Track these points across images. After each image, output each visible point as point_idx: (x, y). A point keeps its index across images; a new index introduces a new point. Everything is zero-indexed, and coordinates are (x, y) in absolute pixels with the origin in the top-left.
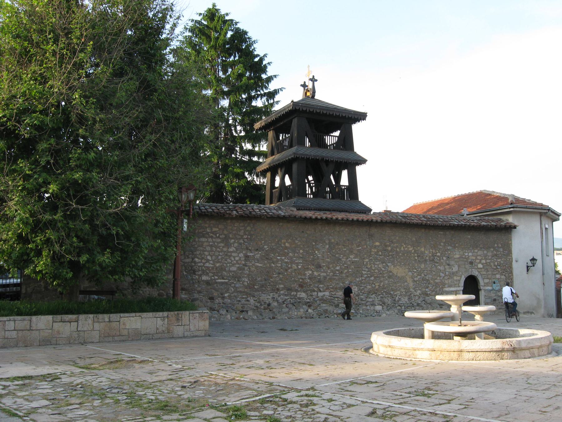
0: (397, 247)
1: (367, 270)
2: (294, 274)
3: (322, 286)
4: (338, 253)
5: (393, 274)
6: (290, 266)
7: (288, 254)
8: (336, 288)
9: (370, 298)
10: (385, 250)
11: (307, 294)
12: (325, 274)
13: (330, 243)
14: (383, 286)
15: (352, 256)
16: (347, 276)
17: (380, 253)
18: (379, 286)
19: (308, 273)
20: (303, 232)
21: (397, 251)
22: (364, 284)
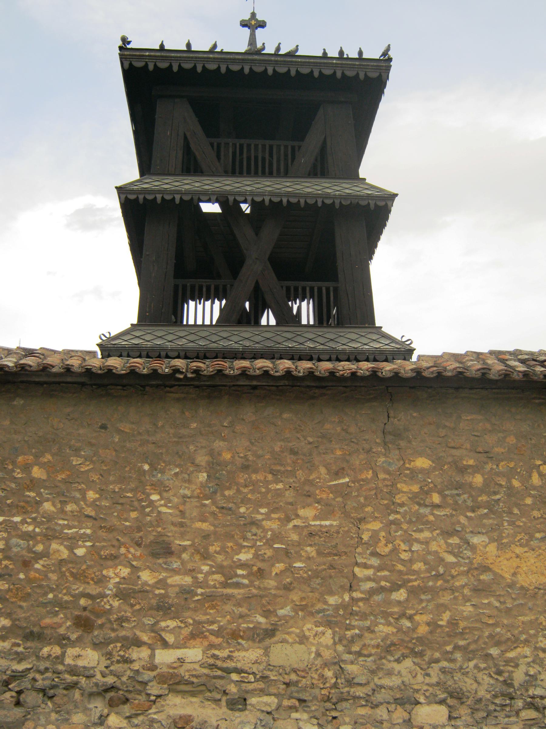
0: (510, 474)
1: (374, 561)
2: (54, 577)
3: (172, 624)
4: (245, 501)
5: (498, 578)
6: (40, 548)
7: (39, 504)
8: (235, 635)
9: (390, 673)
10: (459, 486)
11: (109, 656)
12: (188, 580)
13: (214, 467)
14: (452, 623)
15: (307, 513)
16: (288, 588)
17: (436, 498)
18: (433, 625)
19: (118, 573)
20: (104, 427)
21: (510, 487)
22: (364, 616)
